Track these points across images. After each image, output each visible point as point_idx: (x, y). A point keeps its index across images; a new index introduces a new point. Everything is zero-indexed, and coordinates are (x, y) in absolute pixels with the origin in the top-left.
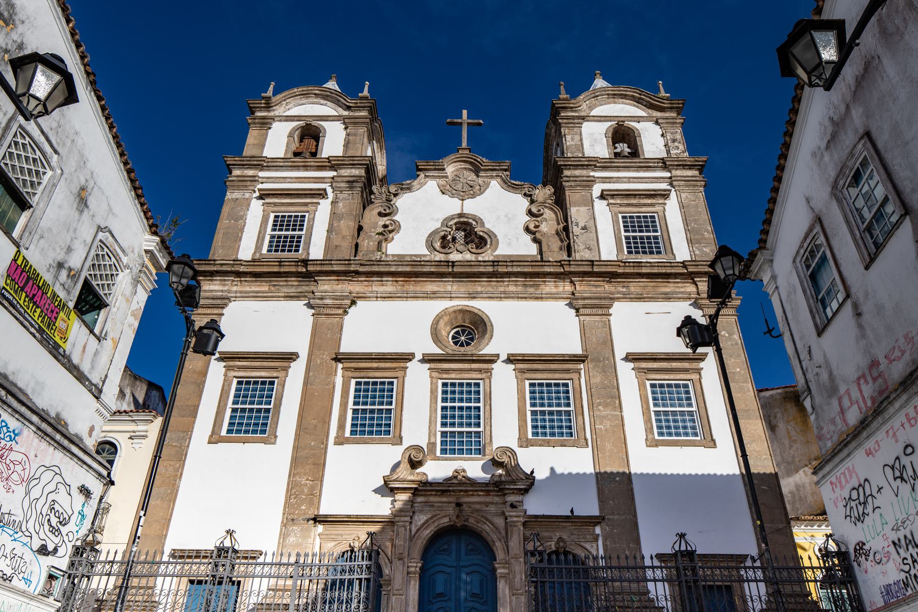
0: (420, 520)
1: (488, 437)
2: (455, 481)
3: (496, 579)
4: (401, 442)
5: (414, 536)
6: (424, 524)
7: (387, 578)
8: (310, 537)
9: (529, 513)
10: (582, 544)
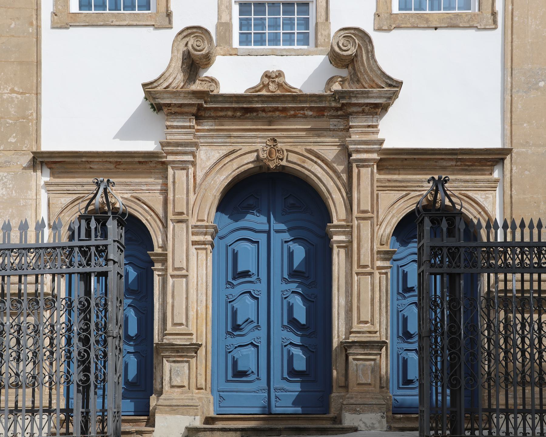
0: (209, 159)
1: (322, 11)
2: (264, 92)
3: (331, 250)
4: (170, 22)
5: (201, 185)
6: (216, 164)
7: (160, 251)
8: (29, 188)
9: (385, 146)
10: (470, 194)
